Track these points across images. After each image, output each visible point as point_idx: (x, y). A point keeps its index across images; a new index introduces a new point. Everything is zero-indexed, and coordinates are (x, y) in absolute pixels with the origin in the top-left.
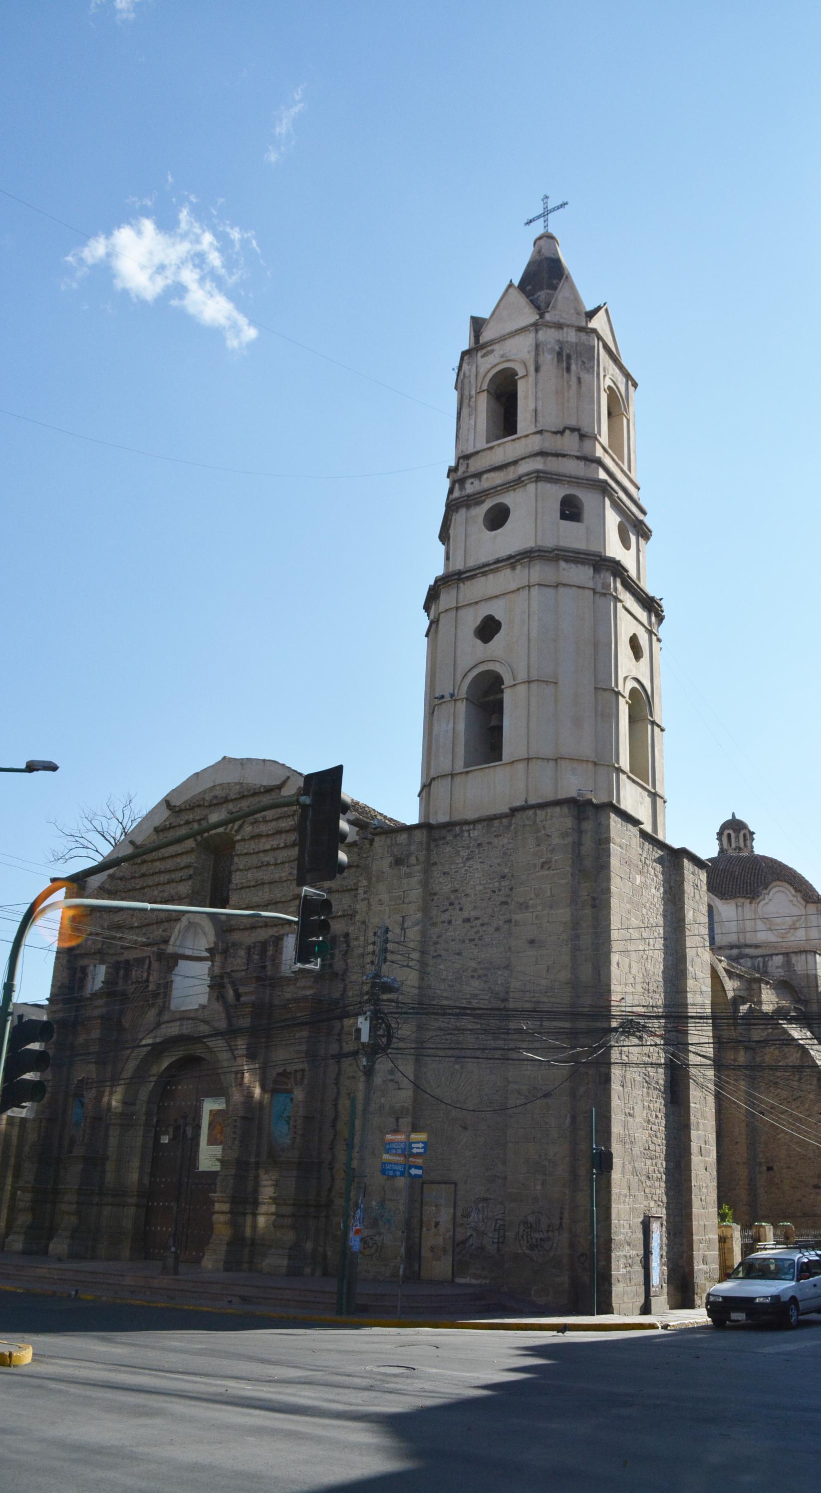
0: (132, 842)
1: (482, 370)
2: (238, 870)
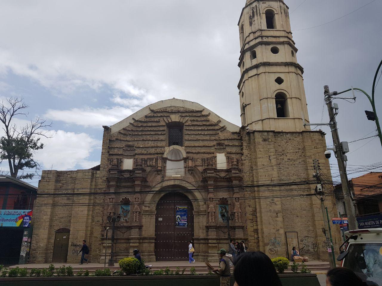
0: (133, 119)
1: (263, 7)
2: (188, 134)
